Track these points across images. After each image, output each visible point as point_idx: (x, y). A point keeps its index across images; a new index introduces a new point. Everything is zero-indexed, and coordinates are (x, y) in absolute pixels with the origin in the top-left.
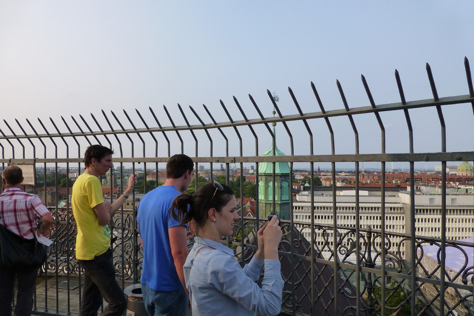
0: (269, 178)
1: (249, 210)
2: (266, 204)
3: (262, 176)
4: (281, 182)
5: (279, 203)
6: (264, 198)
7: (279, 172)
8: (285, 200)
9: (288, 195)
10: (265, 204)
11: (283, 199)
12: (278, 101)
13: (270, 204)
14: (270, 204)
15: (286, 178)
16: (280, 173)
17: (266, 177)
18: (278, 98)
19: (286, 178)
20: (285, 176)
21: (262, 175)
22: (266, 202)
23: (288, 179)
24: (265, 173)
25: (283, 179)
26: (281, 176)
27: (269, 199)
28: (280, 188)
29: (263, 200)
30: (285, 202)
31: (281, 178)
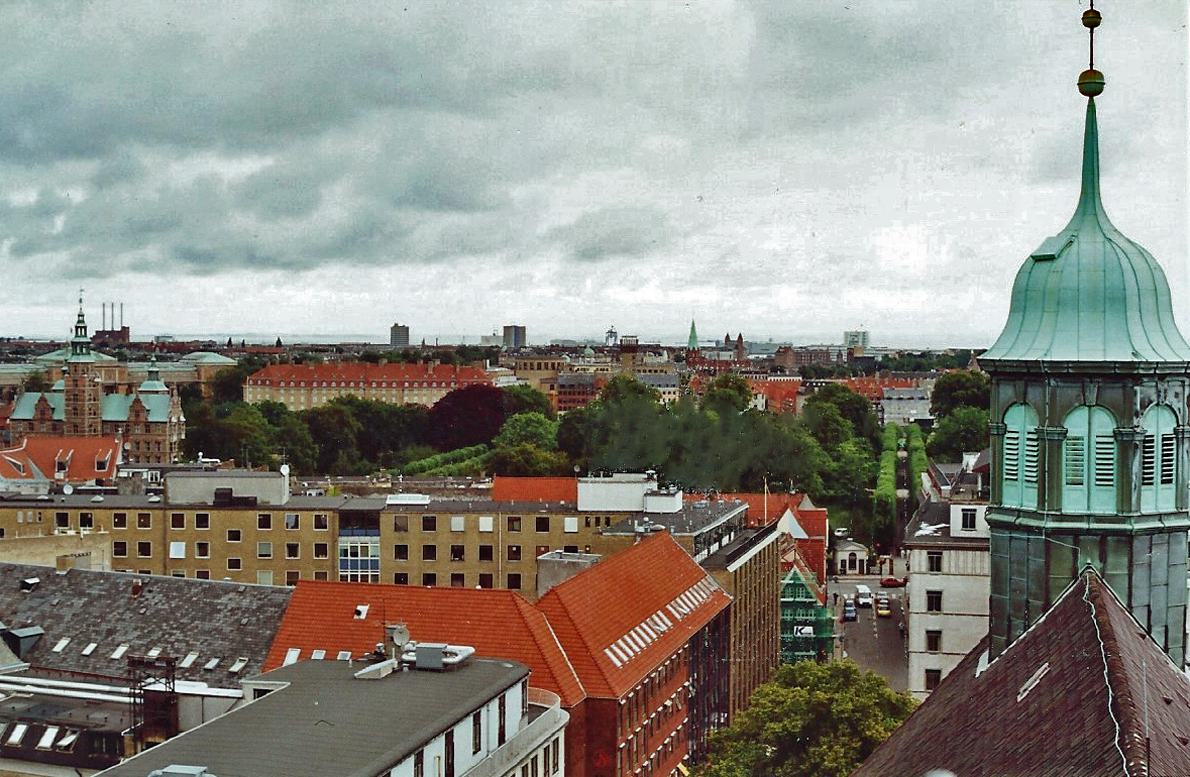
1: (790, 557)
8: (1160, 517)
19: (1165, 391)
20: (1162, 377)
23: (1177, 395)
27: (1068, 509)
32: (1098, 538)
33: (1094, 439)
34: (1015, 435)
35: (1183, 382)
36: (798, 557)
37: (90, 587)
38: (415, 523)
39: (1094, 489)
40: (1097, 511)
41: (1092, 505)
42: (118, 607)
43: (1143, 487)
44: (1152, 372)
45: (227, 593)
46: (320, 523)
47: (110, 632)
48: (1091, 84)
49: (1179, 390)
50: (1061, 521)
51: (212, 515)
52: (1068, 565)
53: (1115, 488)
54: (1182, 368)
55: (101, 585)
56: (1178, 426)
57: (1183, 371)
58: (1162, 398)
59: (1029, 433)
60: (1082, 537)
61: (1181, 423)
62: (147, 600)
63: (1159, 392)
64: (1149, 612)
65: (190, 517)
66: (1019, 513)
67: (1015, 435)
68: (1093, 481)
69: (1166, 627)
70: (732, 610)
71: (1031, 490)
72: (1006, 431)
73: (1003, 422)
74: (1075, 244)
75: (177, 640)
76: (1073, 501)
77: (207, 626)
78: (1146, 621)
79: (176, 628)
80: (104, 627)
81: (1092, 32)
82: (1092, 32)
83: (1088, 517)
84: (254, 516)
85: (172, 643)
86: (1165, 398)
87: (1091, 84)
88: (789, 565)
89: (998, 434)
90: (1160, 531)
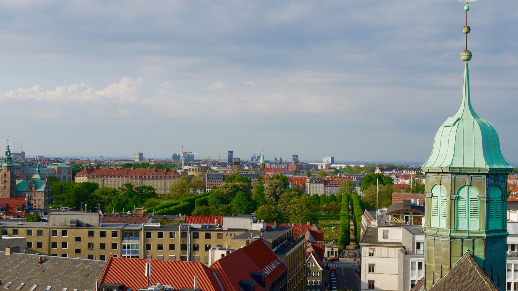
2: (451, 238)
3: (441, 174)
4: (487, 189)
5: (483, 237)
6: (446, 227)
7: (483, 166)
8: (496, 231)
9: (501, 219)
10: (449, 239)
11: (491, 228)
16: (488, 167)
19: (498, 180)
20: (497, 174)
21: (443, 173)
22: (452, 235)
23: (502, 182)
27: (459, 229)
29: (445, 230)
31: (487, 179)
32: (472, 240)
33: (470, 200)
34: (436, 198)
35: (504, 176)
36: (312, 250)
37: (20, 260)
38: (154, 234)
39: (470, 219)
41: (469, 228)
42: (32, 269)
43: (489, 219)
45: (79, 263)
46: (115, 234)
47: (29, 279)
49: (503, 180)
50: (456, 233)
51: (69, 231)
52: (459, 251)
53: (478, 219)
54: (504, 171)
55: (25, 259)
56: (503, 194)
58: (496, 183)
60: (464, 240)
61: (503, 193)
62: (45, 266)
63: (495, 180)
64: (492, 271)
65: (59, 232)
67: (436, 198)
68: (470, 217)
69: (498, 277)
70: (288, 271)
71: (444, 220)
72: (432, 196)
73: (431, 193)
75: (58, 283)
77: (70, 277)
78: (491, 275)
79: (58, 278)
80: (27, 277)
84: (86, 231)
85: (56, 284)
86: (498, 183)
88: (310, 253)
89: (429, 197)
90: (496, 237)
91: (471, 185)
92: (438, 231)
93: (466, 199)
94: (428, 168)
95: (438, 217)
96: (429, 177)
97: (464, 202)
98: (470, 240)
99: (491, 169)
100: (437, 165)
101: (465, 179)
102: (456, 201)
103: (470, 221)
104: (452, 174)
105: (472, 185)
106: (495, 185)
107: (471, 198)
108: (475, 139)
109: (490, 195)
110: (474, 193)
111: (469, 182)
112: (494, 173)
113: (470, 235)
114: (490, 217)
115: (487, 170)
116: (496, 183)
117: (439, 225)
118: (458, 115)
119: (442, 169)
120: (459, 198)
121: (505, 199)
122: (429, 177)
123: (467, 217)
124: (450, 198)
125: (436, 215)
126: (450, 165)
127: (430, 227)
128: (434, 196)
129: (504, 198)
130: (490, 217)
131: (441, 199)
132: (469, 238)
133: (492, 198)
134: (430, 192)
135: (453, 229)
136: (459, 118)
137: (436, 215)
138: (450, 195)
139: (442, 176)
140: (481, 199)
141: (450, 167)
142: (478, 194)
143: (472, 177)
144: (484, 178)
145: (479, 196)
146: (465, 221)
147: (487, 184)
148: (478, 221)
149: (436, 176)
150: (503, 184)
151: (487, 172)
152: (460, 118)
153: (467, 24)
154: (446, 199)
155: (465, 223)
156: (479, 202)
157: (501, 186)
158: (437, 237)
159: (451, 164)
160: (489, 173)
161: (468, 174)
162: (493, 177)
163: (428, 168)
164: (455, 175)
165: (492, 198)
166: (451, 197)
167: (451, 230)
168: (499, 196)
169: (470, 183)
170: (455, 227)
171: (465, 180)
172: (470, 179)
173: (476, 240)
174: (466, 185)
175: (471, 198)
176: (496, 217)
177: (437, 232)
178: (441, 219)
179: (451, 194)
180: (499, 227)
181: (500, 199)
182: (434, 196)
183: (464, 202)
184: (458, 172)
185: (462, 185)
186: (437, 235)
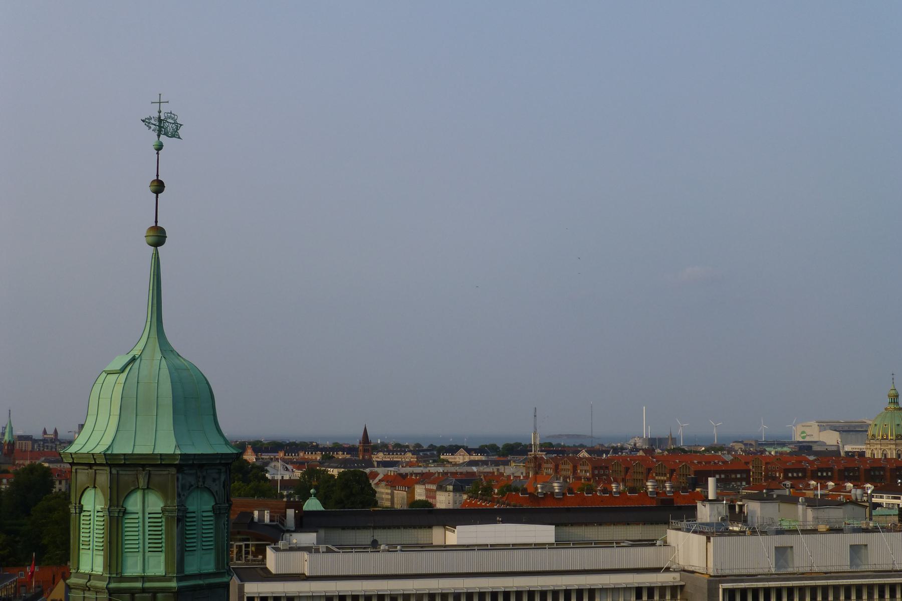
0: (126, 476)
3: (95, 468)
6: (102, 571)
7: (170, 451)
9: (213, 551)
12: (175, 135)
13: (133, 594)
14: (133, 594)
15: (204, 477)
16: (178, 452)
17: (114, 471)
18: (178, 126)
19: (204, 477)
20: (201, 466)
21: (96, 464)
22: (113, 585)
24: (109, 452)
25: (191, 480)
26: (180, 468)
28: (179, 520)
29: (99, 578)
30: (201, 582)
31: (180, 476)
32: (150, 595)
33: (147, 516)
34: (88, 514)
39: (147, 554)
40: (150, 572)
41: (147, 571)
43: (186, 553)
44: (191, 462)
48: (158, 237)
50: (120, 582)
56: (216, 504)
57: (218, 462)
58: (200, 484)
59: (98, 512)
60: (136, 595)
66: (90, 576)
67: (88, 514)
68: (147, 550)
72: (81, 510)
74: (138, 361)
76: (133, 567)
81: (157, 197)
82: (157, 197)
83: (144, 579)
86: (204, 483)
87: (158, 237)
91: (148, 488)
92: (89, 580)
93: (140, 515)
94: (71, 455)
95: (90, 552)
96: (76, 472)
97: (136, 521)
98: (147, 595)
99: (184, 456)
100: (85, 451)
101: (138, 476)
102: (120, 518)
103: (148, 557)
104: (111, 466)
105: (149, 487)
106: (198, 487)
107: (149, 513)
108: (159, 399)
109: (187, 507)
110: (156, 503)
111: (144, 482)
112: (193, 462)
113: (147, 585)
114: (187, 549)
115: (177, 457)
116: (200, 484)
117: (91, 568)
118: (136, 352)
119: (95, 457)
120: (125, 512)
121: (220, 513)
122: (76, 472)
123: (141, 550)
124: (108, 513)
125: (87, 547)
126: (108, 449)
127: (77, 572)
128: (84, 511)
129: (218, 512)
130: (187, 549)
131: (95, 516)
132: (144, 590)
133: (194, 512)
134: (78, 502)
135: (114, 576)
136: (134, 356)
137: (87, 547)
138: (107, 507)
139: (97, 471)
140: (167, 514)
141: (107, 453)
142: (162, 505)
143: (150, 471)
144: (173, 473)
145: (164, 511)
146: (139, 558)
147: (180, 486)
148: (162, 556)
149: (87, 471)
150: (216, 485)
151: (177, 462)
152: (137, 356)
153: (158, 176)
154: (104, 516)
155: (139, 561)
156: (164, 520)
157: (211, 489)
158: (88, 592)
159: (109, 447)
160: (181, 463)
161: (143, 466)
162: (194, 471)
163: (71, 455)
164: (118, 469)
165: (194, 512)
166: (109, 512)
167: (110, 577)
168: (209, 507)
169: (146, 483)
170: (119, 571)
171: (137, 478)
172: (147, 476)
173: (159, 595)
174: (138, 488)
175: (149, 513)
176: (203, 549)
177: (87, 581)
178: (97, 555)
179: (110, 506)
180: (210, 568)
181: (211, 514)
182: (84, 511)
183: (136, 521)
184: (123, 462)
185: (133, 488)
186: (87, 586)
